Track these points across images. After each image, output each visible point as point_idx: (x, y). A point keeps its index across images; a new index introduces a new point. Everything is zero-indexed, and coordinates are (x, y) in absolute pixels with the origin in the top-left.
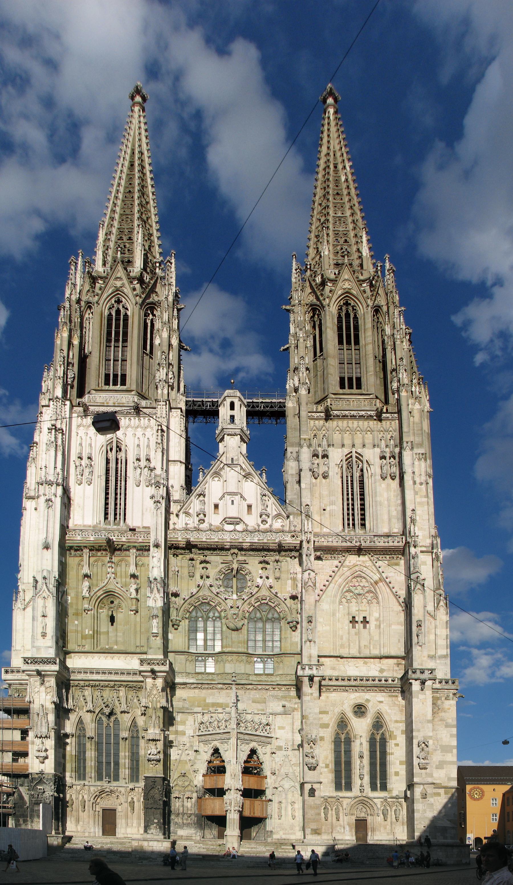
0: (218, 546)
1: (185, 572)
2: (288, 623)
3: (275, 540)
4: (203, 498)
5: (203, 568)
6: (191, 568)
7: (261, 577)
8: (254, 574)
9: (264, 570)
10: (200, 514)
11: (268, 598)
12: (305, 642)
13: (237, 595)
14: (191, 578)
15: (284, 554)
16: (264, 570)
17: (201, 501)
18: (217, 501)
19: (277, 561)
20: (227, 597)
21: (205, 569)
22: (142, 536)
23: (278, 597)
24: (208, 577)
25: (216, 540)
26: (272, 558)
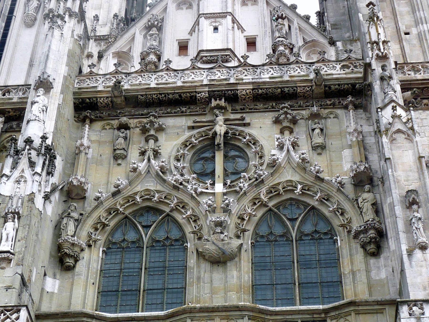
0: (183, 96)
1: (107, 152)
2: (356, 236)
3: (307, 75)
4: (157, 33)
5: (147, 141)
6: (121, 140)
7: (281, 147)
8: (263, 142)
9: (287, 133)
10: (148, 54)
11: (299, 187)
12: (410, 253)
13: (225, 184)
14: (120, 161)
15: (329, 103)
16: (287, 133)
17: (151, 35)
18: (184, 36)
19: (314, 116)
20: (200, 190)
21: (151, 142)
22: (21, 93)
23: (322, 180)
24: (156, 154)
25: (179, 84)
26: (304, 112)
